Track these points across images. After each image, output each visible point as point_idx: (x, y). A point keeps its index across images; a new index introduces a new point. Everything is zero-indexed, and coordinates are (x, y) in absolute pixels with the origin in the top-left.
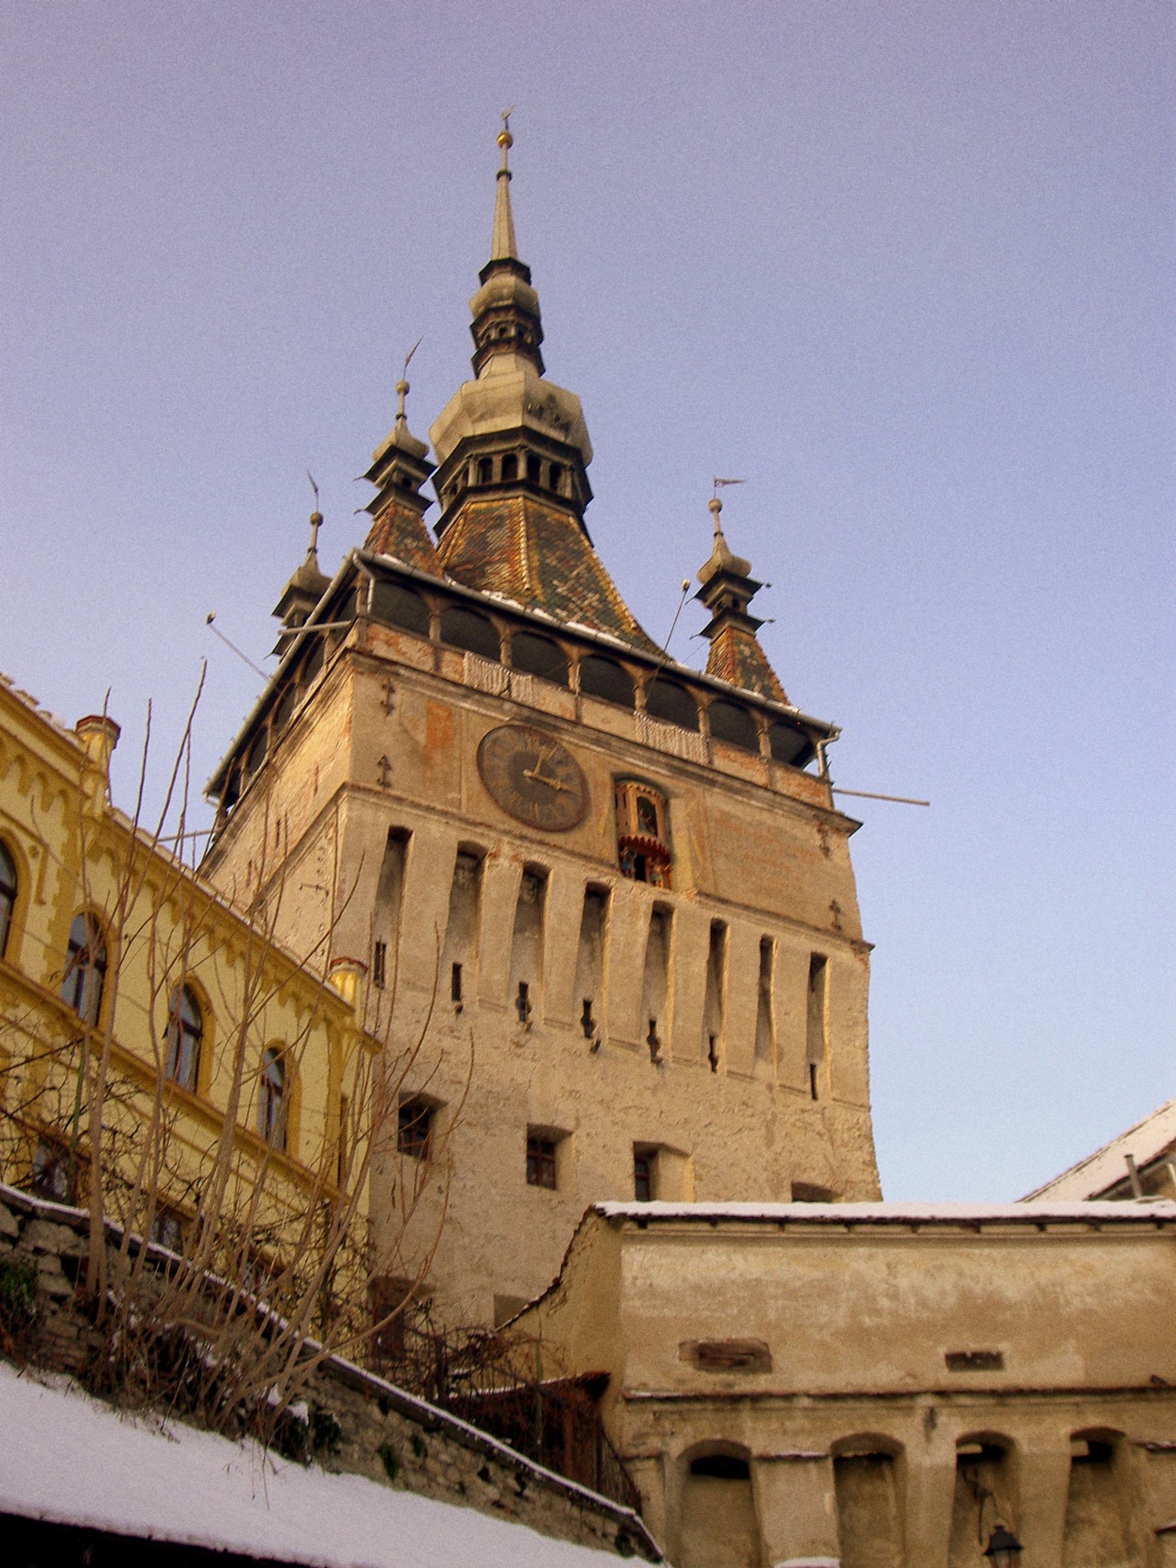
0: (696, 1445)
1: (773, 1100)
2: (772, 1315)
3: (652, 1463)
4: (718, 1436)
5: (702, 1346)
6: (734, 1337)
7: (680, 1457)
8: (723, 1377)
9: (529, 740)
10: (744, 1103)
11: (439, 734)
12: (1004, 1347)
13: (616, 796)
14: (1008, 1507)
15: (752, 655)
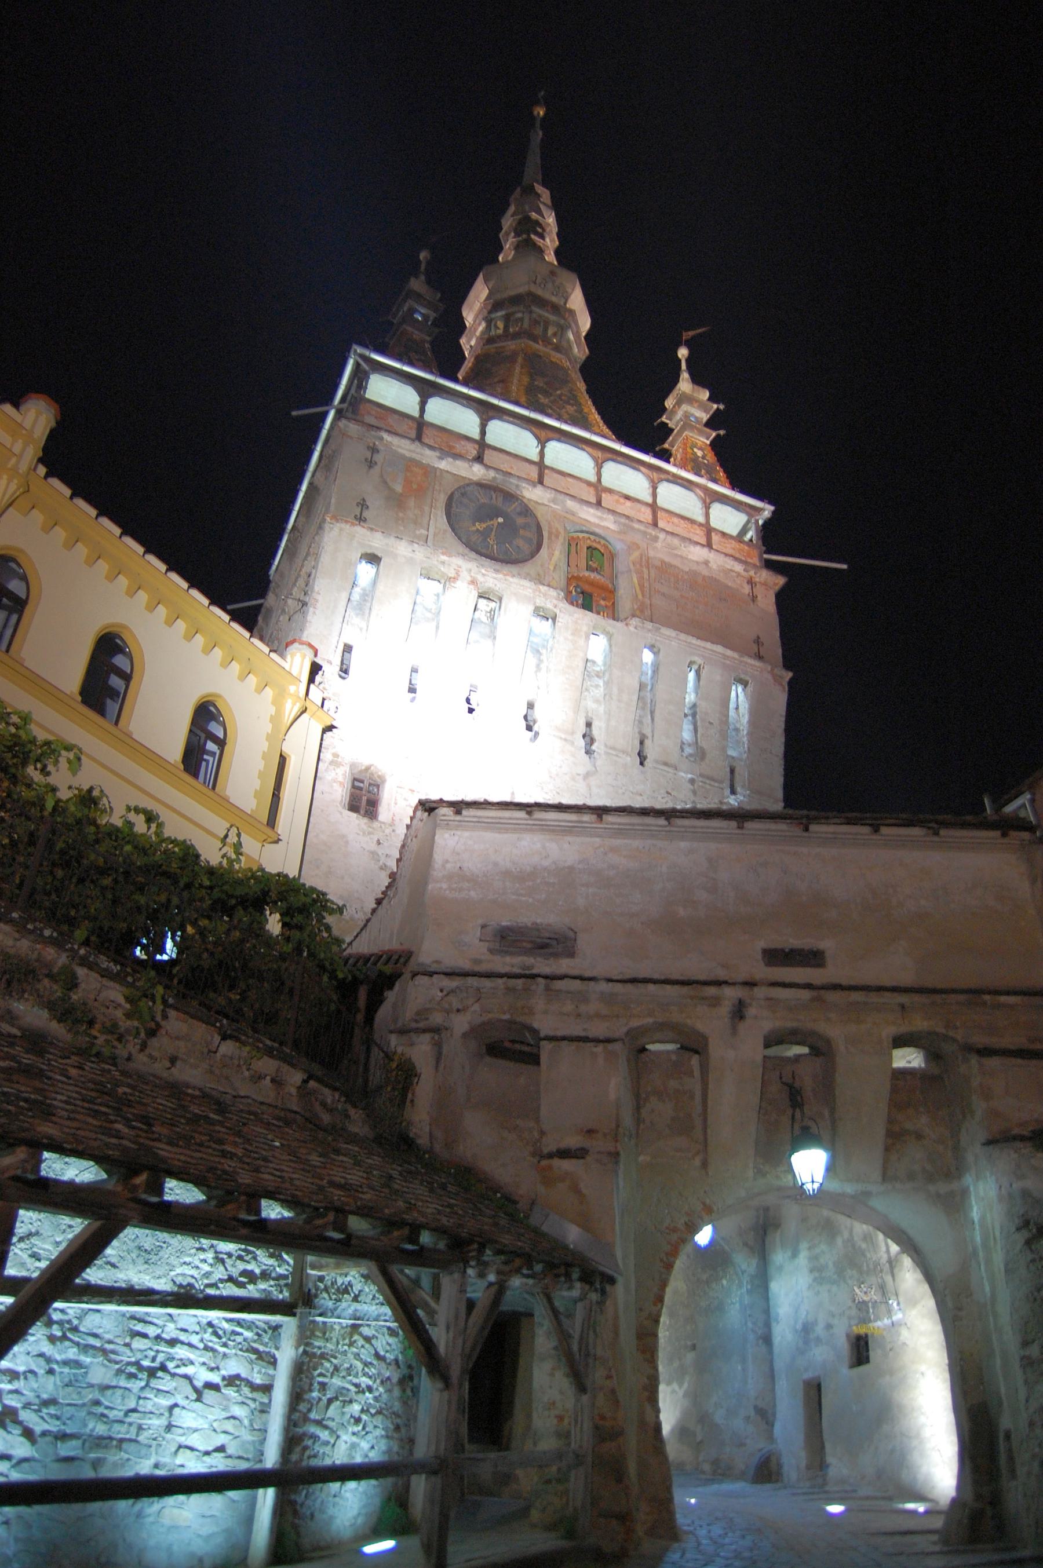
0: (484, 1024)
1: (694, 792)
2: (581, 902)
3: (426, 1037)
4: (507, 1017)
5: (508, 928)
6: (539, 921)
7: (465, 1035)
8: (529, 960)
9: (494, 497)
10: (668, 793)
11: (415, 486)
12: (826, 944)
13: (570, 545)
14: (826, 1113)
15: (704, 457)
